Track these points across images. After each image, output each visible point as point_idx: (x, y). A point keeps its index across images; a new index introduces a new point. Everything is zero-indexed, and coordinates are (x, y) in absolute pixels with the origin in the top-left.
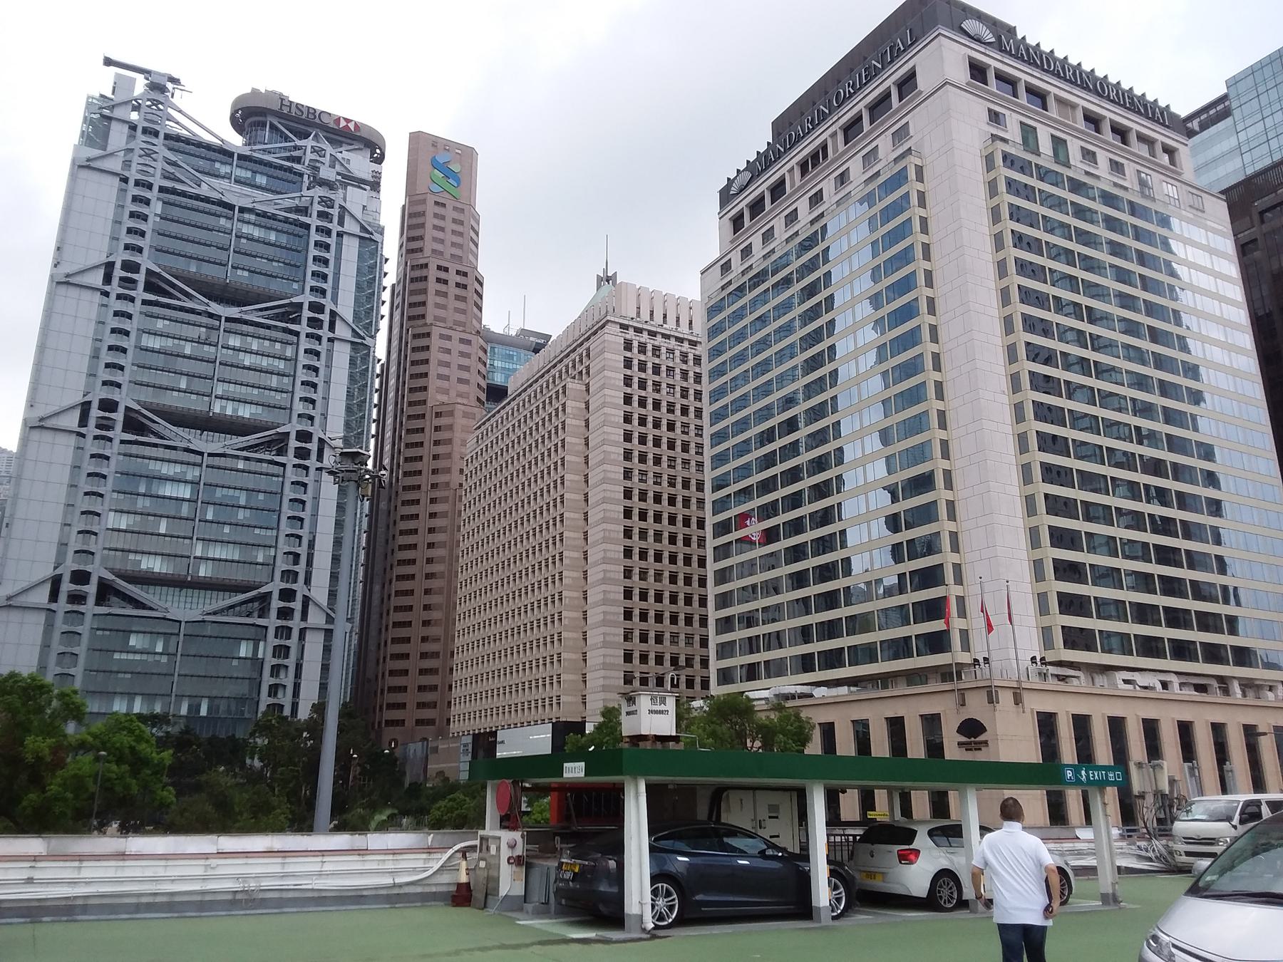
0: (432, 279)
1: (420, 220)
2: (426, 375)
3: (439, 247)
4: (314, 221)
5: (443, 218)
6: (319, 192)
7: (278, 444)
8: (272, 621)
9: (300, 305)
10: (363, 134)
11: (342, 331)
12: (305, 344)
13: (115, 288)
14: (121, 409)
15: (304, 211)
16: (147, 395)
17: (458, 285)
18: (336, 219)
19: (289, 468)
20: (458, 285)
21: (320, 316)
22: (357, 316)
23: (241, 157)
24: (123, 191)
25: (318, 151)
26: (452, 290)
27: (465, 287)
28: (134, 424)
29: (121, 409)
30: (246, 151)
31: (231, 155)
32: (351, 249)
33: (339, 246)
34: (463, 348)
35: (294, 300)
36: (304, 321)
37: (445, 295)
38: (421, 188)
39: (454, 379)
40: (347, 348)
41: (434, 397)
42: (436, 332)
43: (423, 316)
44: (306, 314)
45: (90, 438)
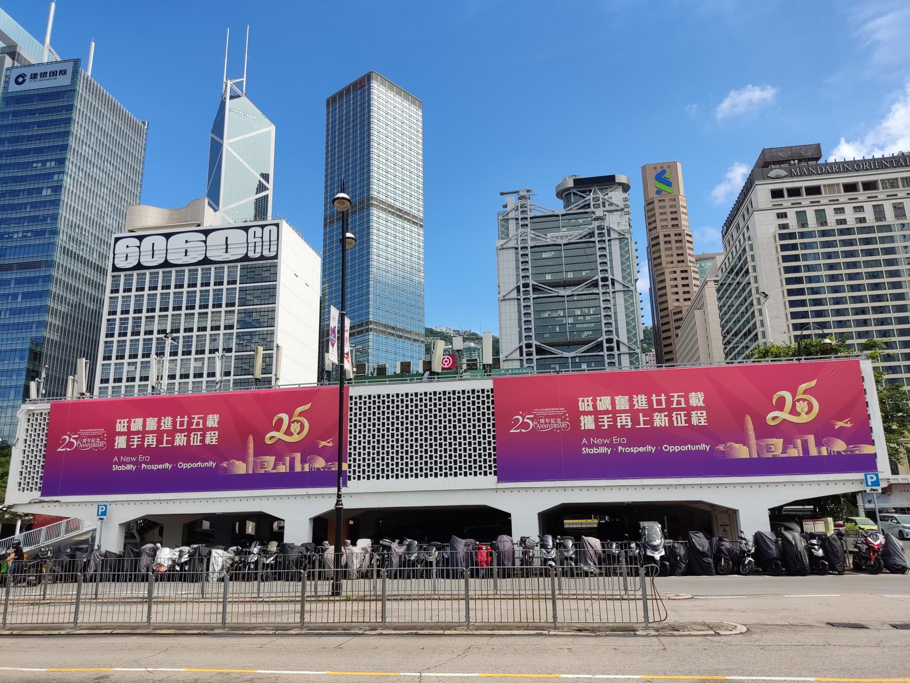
0: (662, 243)
2: (666, 294)
4: (596, 239)
5: (664, 207)
6: (596, 224)
7: (599, 346)
11: (618, 287)
13: (522, 297)
15: (592, 234)
17: (677, 241)
19: (606, 357)
20: (677, 241)
22: (624, 278)
25: (596, 199)
26: (674, 245)
27: (681, 241)
28: (540, 351)
30: (564, 212)
32: (616, 245)
33: (610, 246)
34: (684, 275)
37: (671, 249)
38: (652, 194)
39: (681, 292)
41: (672, 305)
42: (667, 271)
43: (660, 264)
44: (600, 283)
45: (525, 361)
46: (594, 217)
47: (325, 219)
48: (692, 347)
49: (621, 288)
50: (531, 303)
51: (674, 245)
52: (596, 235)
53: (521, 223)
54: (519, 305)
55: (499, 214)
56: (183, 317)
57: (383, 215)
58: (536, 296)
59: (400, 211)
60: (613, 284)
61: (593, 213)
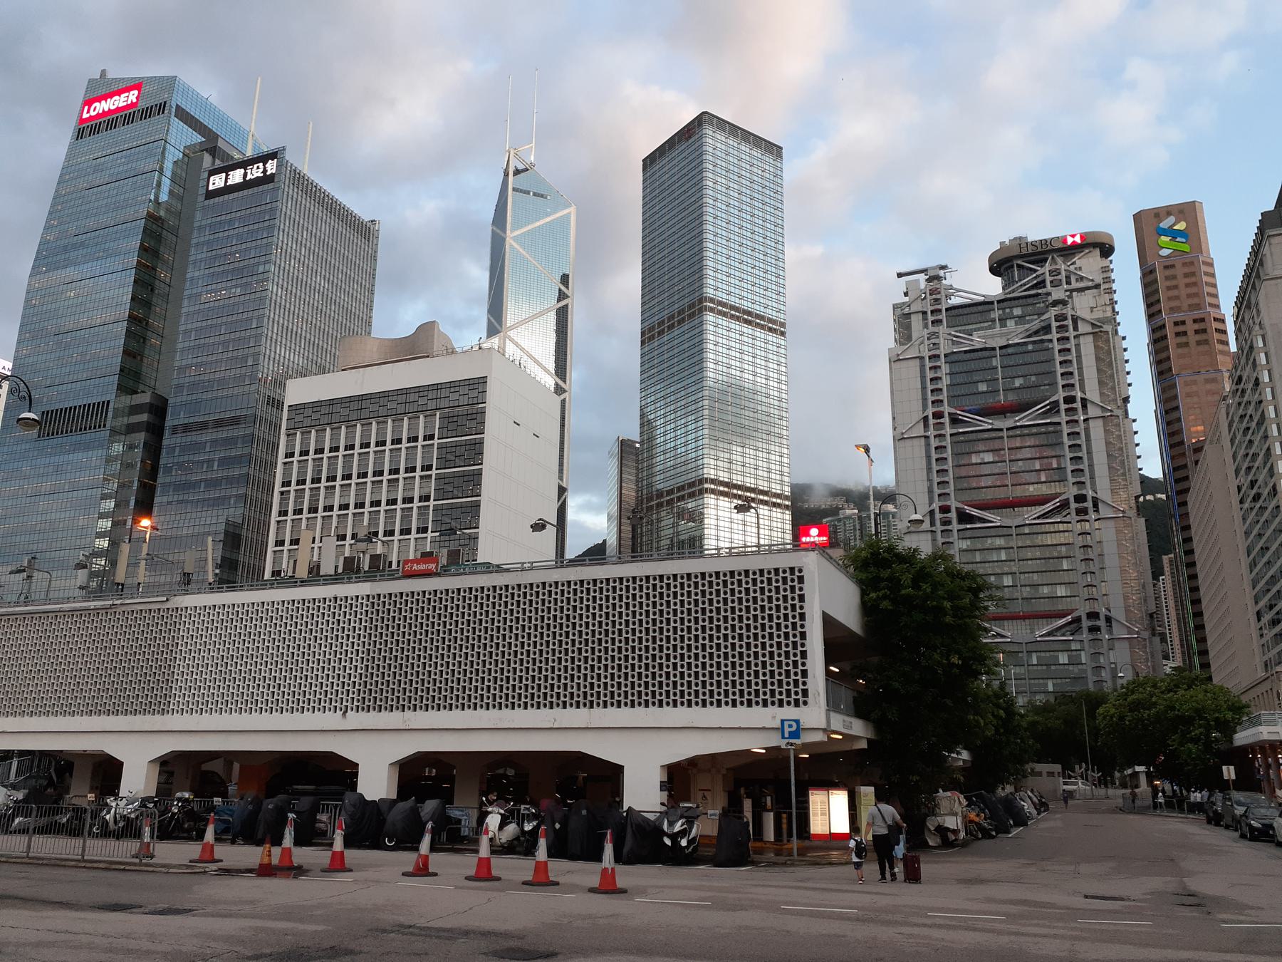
1: (1154, 288)
3: (1174, 304)
4: (1054, 335)
5: (1174, 277)
6: (1053, 311)
8: (1085, 635)
9: (1057, 402)
10: (1089, 241)
11: (1092, 412)
12: (1066, 430)
13: (931, 433)
14: (953, 510)
15: (1047, 329)
16: (968, 496)
17: (1197, 332)
18: (1071, 328)
20: (1197, 332)
21: (1074, 405)
22: (1102, 394)
23: (999, 302)
24: (922, 366)
26: (1192, 338)
27: (1204, 331)
28: (964, 517)
29: (953, 510)
31: (992, 303)
32: (1088, 346)
35: (1052, 400)
36: (1063, 413)
40: (1100, 422)
44: (1063, 407)
45: (939, 534)
46: (1050, 299)
47: (643, 334)
48: (1208, 505)
49: (1099, 413)
50: (948, 442)
51: (1192, 338)
52: (1054, 330)
53: (930, 318)
54: (928, 445)
55: (895, 307)
56: (369, 485)
57: (722, 321)
58: (955, 431)
59: (749, 313)
60: (1084, 406)
61: (1049, 294)
